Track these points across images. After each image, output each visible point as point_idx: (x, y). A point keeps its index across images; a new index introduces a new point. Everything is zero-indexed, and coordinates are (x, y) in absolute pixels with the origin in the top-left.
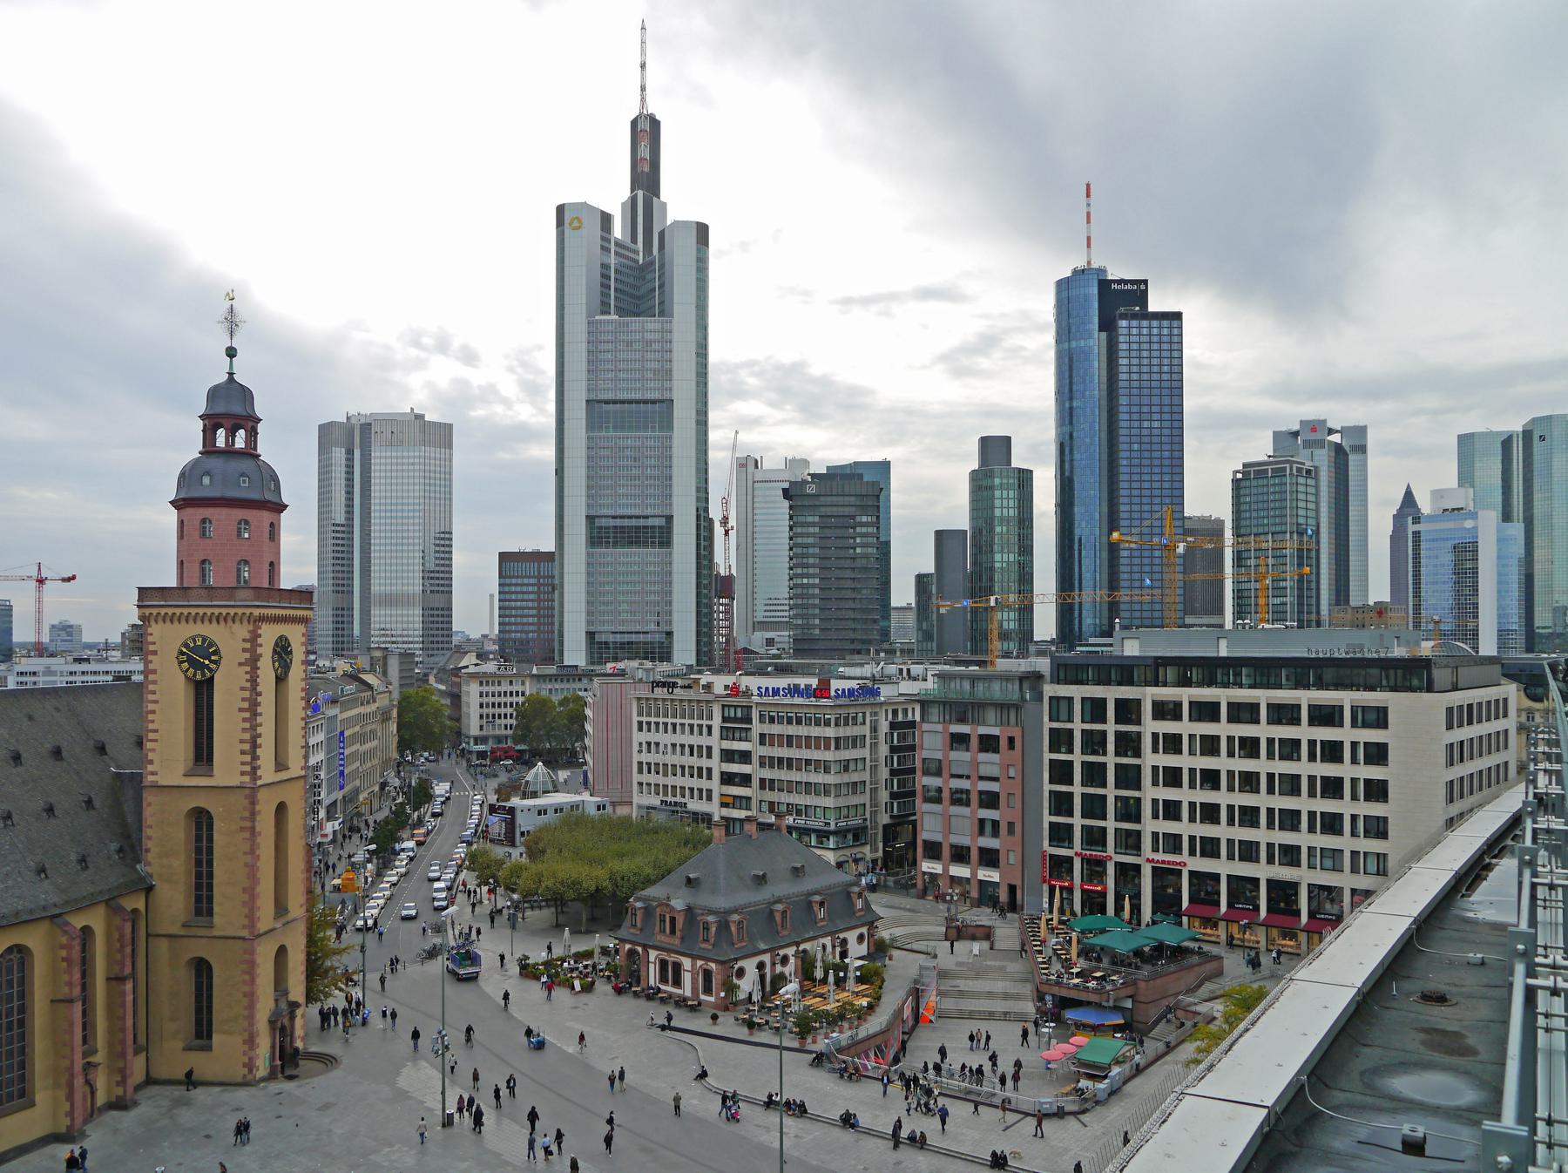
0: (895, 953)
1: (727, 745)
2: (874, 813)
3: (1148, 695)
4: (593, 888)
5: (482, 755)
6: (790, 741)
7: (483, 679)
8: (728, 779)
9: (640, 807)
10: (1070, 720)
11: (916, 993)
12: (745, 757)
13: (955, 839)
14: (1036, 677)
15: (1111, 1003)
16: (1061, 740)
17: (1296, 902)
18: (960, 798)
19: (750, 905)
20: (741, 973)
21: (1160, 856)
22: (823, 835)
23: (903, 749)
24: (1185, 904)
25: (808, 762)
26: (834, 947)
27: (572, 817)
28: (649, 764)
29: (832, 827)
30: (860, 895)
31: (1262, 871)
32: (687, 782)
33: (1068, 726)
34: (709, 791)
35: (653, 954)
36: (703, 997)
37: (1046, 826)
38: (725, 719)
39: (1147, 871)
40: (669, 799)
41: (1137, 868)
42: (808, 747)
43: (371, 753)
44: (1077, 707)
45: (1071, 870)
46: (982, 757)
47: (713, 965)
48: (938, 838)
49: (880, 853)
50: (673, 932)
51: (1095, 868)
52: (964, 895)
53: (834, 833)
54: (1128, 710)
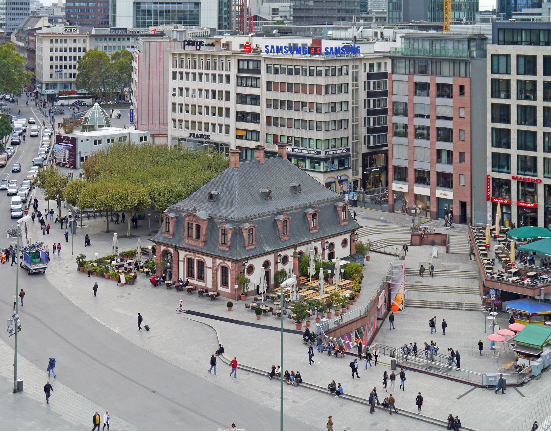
4: (136, 202)
7: (53, 38)
8: (242, 117)
9: (173, 138)
11: (388, 287)
12: (255, 100)
13: (418, 165)
15: (542, 297)
19: (258, 216)
20: (251, 269)
23: (377, 95)
25: (304, 104)
26: (324, 249)
27: (120, 146)
28: (181, 105)
29: (323, 155)
30: (344, 209)
32: (210, 119)
34: (227, 126)
35: (182, 254)
38: (240, 70)
40: (197, 132)
42: (304, 92)
45: (509, 191)
46: (439, 101)
47: (229, 264)
49: (360, 176)
50: (198, 237)
52: (426, 210)
53: (325, 160)
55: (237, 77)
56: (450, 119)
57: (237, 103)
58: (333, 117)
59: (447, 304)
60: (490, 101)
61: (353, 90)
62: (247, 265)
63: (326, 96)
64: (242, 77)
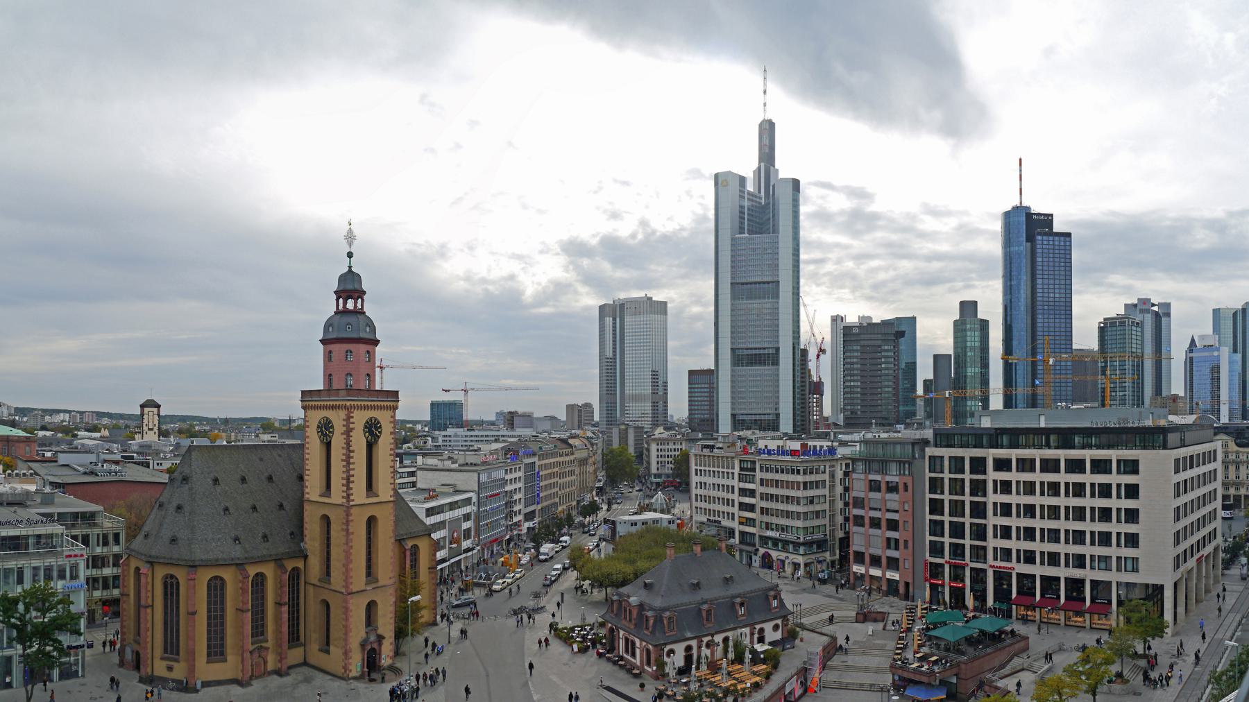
0: (804, 634)
1: (742, 485)
2: (832, 531)
3: (991, 454)
5: (658, 484)
6: (777, 483)
7: (660, 441)
8: (743, 507)
10: (942, 472)
12: (752, 493)
14: (925, 442)
16: (935, 485)
17: (1083, 592)
18: (875, 523)
19: (682, 605)
21: (999, 563)
22: (797, 545)
24: (1014, 595)
29: (802, 540)
30: (775, 598)
31: (1062, 572)
33: (941, 475)
35: (622, 633)
37: (927, 543)
38: (741, 469)
39: (990, 574)
41: (985, 571)
43: (571, 484)
44: (946, 463)
46: (889, 496)
48: (862, 549)
49: (837, 557)
51: (957, 574)
53: (803, 544)
54: (978, 465)
56: (897, 511)
58: (811, 508)
59: (862, 685)
60: (928, 496)
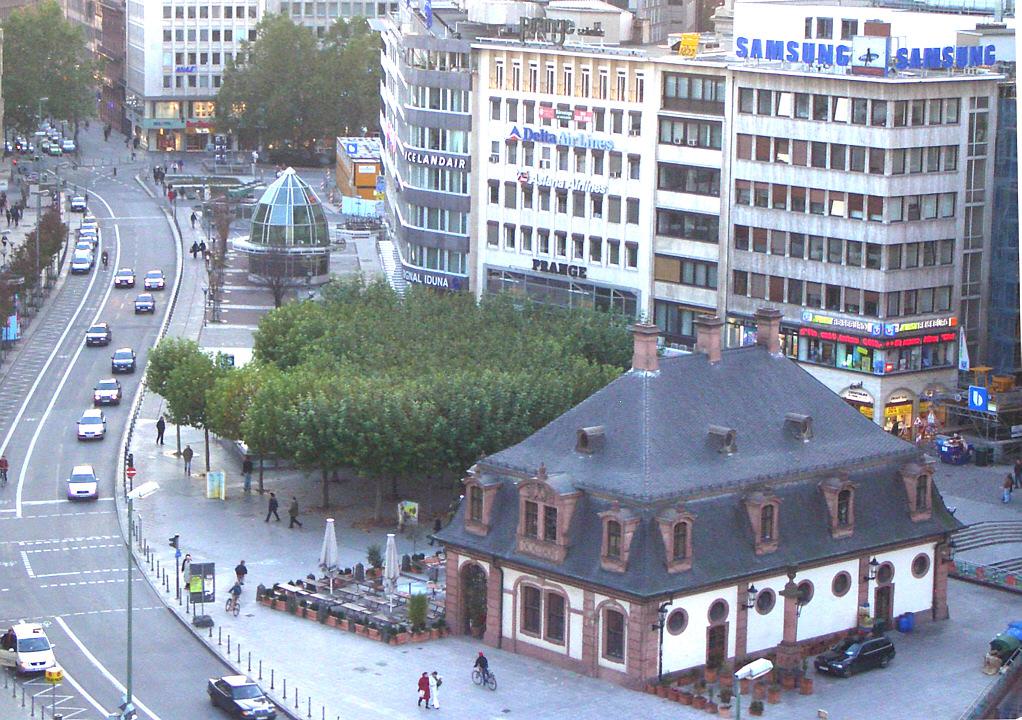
8: (672, 223)
12: (707, 181)
20: (679, 621)
26: (864, 580)
34: (633, 248)
35: (511, 577)
36: (604, 662)
38: (667, 101)
40: (552, 257)
47: (626, 606)
50: (551, 532)
55: (661, 119)
57: (659, 188)
58: (913, 233)
61: (970, 162)
62: (670, 609)
63: (897, 182)
64: (673, 120)
